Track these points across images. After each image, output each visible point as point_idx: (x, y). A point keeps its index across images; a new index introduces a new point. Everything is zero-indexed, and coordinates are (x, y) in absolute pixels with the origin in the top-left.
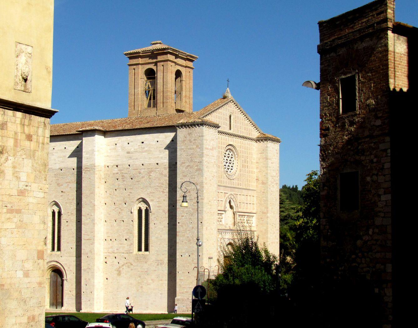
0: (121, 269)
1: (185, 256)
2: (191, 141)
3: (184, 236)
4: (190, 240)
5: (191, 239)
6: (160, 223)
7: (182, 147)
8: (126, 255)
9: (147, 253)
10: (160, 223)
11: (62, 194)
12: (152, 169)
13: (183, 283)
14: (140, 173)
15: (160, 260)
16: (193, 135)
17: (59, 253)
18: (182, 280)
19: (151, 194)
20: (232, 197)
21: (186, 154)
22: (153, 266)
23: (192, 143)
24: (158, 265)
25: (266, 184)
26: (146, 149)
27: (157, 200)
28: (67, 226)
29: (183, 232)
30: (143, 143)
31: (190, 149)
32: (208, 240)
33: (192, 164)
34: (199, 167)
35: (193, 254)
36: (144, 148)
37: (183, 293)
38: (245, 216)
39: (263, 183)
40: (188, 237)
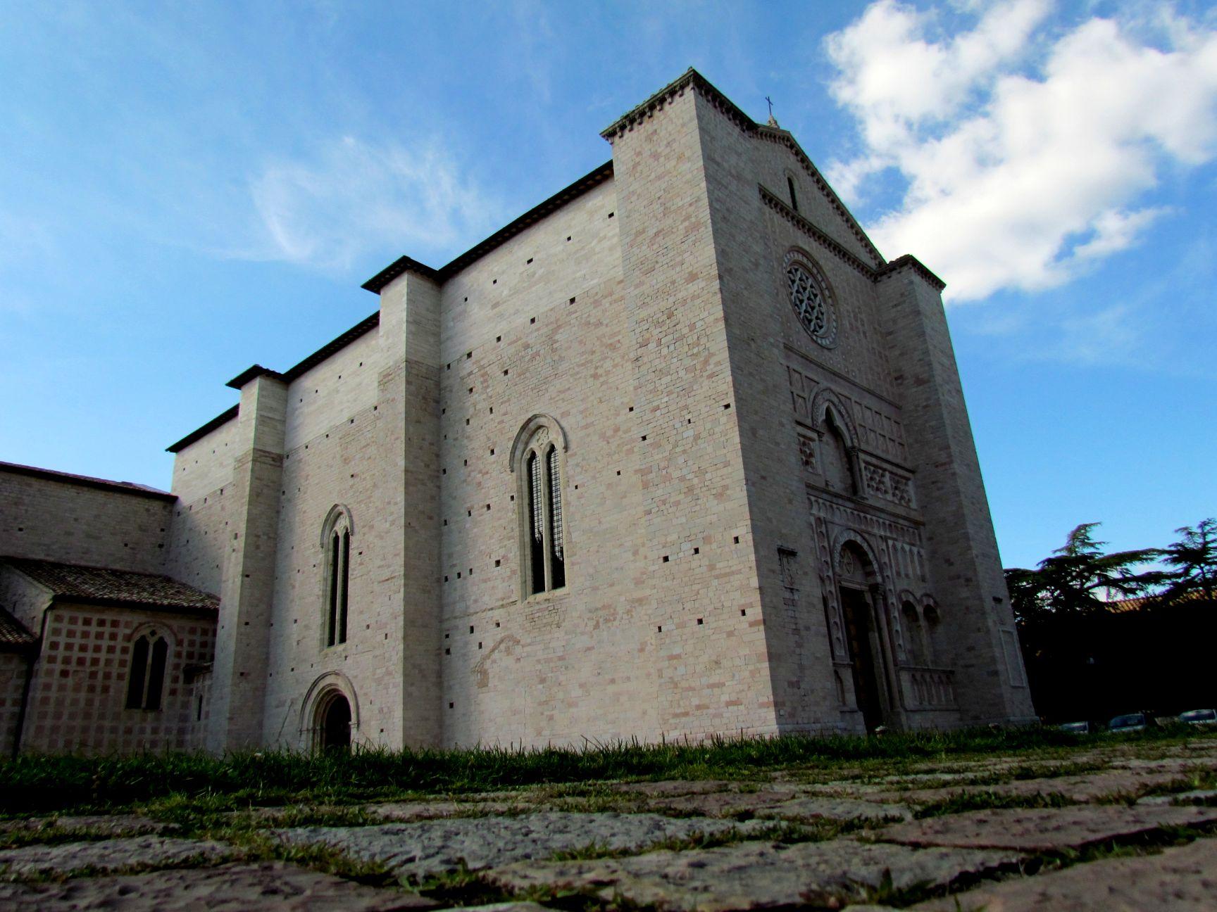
0: (488, 664)
1: (681, 555)
2: (656, 156)
3: (668, 478)
4: (690, 490)
5: (696, 481)
6: (594, 477)
7: (631, 189)
8: (498, 615)
9: (559, 592)
10: (594, 477)
11: (356, 479)
12: (557, 320)
13: (681, 670)
14: (527, 346)
15: (604, 607)
16: (663, 133)
17: (343, 646)
18: (678, 657)
19: (562, 396)
20: (836, 400)
21: (645, 203)
22: (582, 633)
23: (662, 159)
24: (597, 626)
25: (928, 381)
26: (541, 272)
27: (581, 408)
28: (361, 564)
29: (662, 465)
30: (530, 261)
31: (659, 178)
32: (764, 478)
33: (669, 221)
34: (693, 220)
35: (707, 540)
36: (534, 273)
37: (686, 714)
38: (885, 470)
39: (919, 382)
40: (682, 479)
